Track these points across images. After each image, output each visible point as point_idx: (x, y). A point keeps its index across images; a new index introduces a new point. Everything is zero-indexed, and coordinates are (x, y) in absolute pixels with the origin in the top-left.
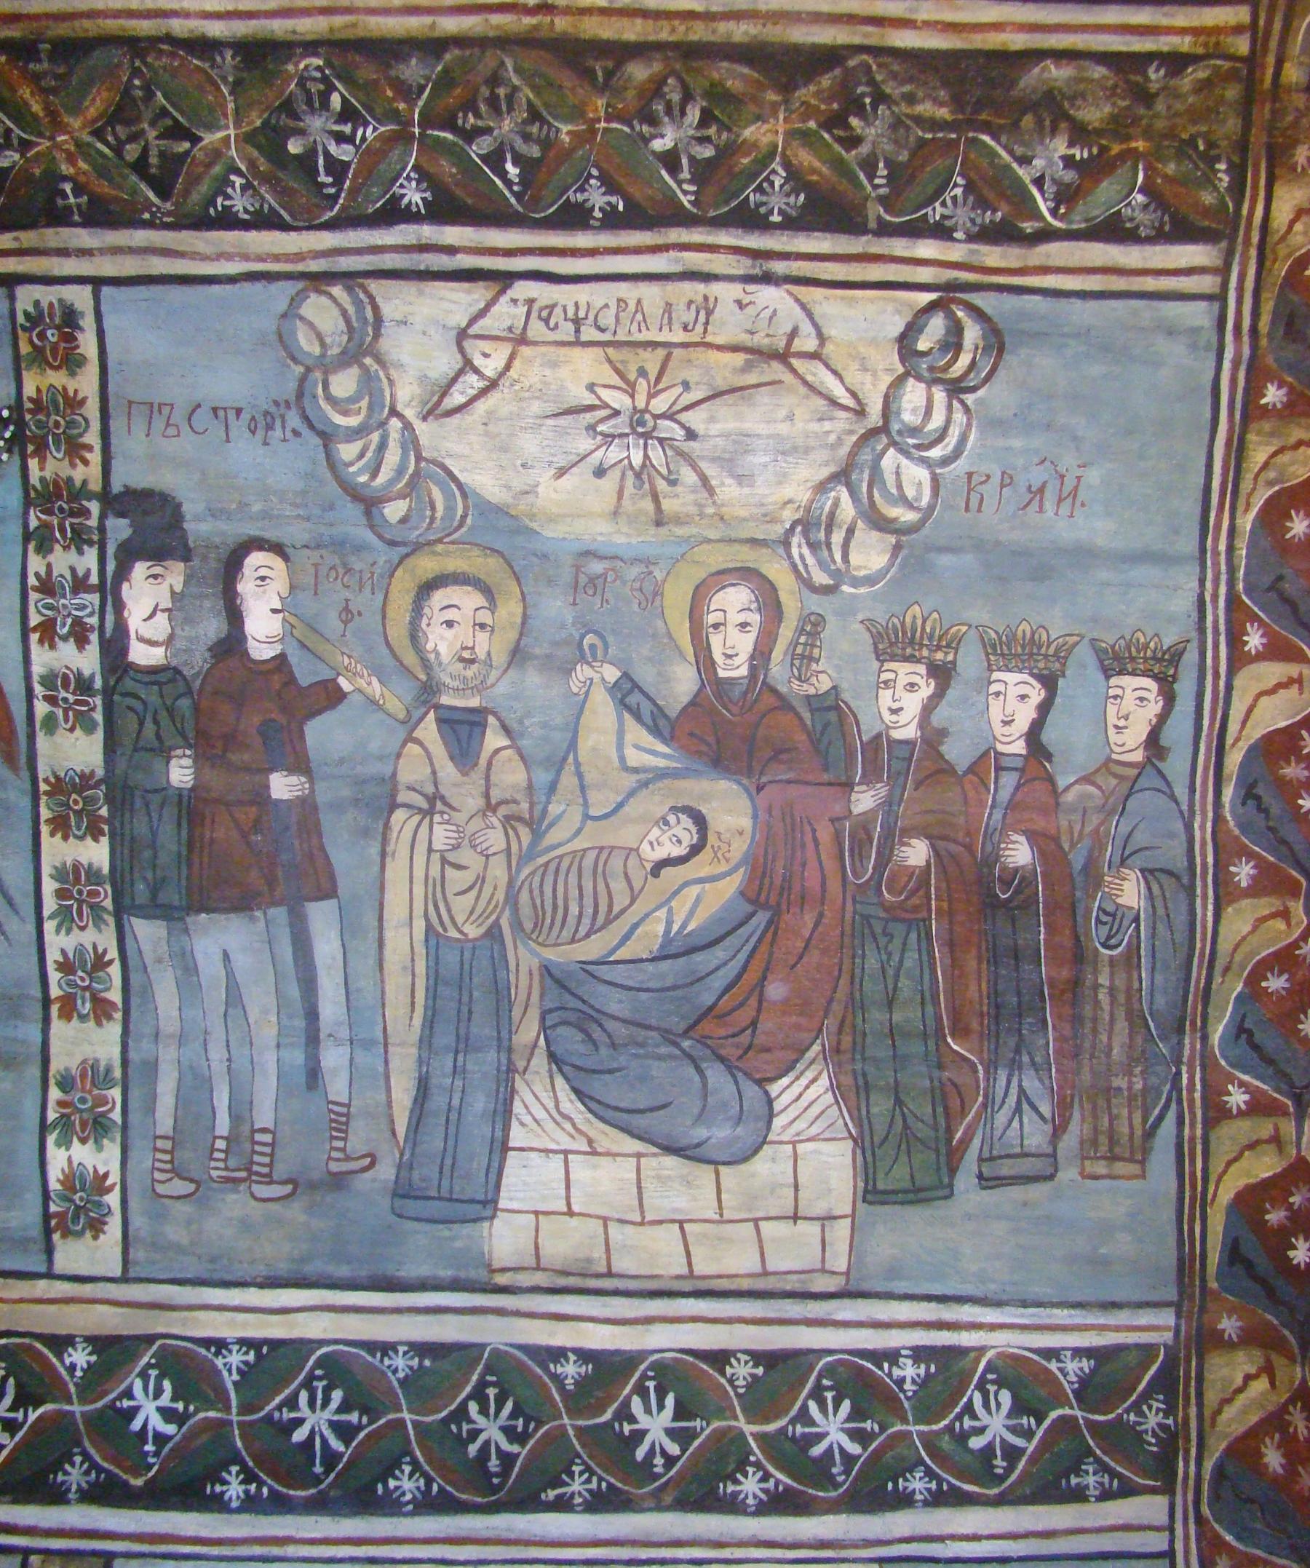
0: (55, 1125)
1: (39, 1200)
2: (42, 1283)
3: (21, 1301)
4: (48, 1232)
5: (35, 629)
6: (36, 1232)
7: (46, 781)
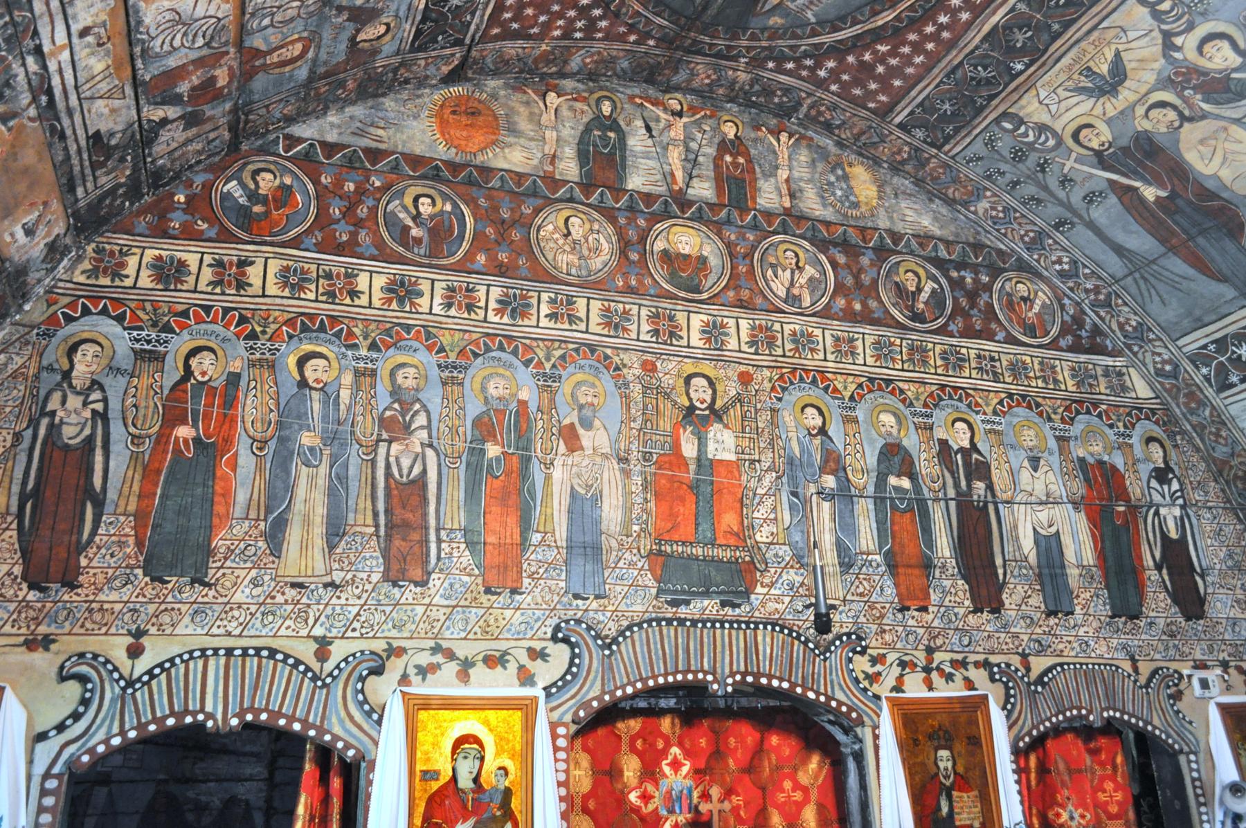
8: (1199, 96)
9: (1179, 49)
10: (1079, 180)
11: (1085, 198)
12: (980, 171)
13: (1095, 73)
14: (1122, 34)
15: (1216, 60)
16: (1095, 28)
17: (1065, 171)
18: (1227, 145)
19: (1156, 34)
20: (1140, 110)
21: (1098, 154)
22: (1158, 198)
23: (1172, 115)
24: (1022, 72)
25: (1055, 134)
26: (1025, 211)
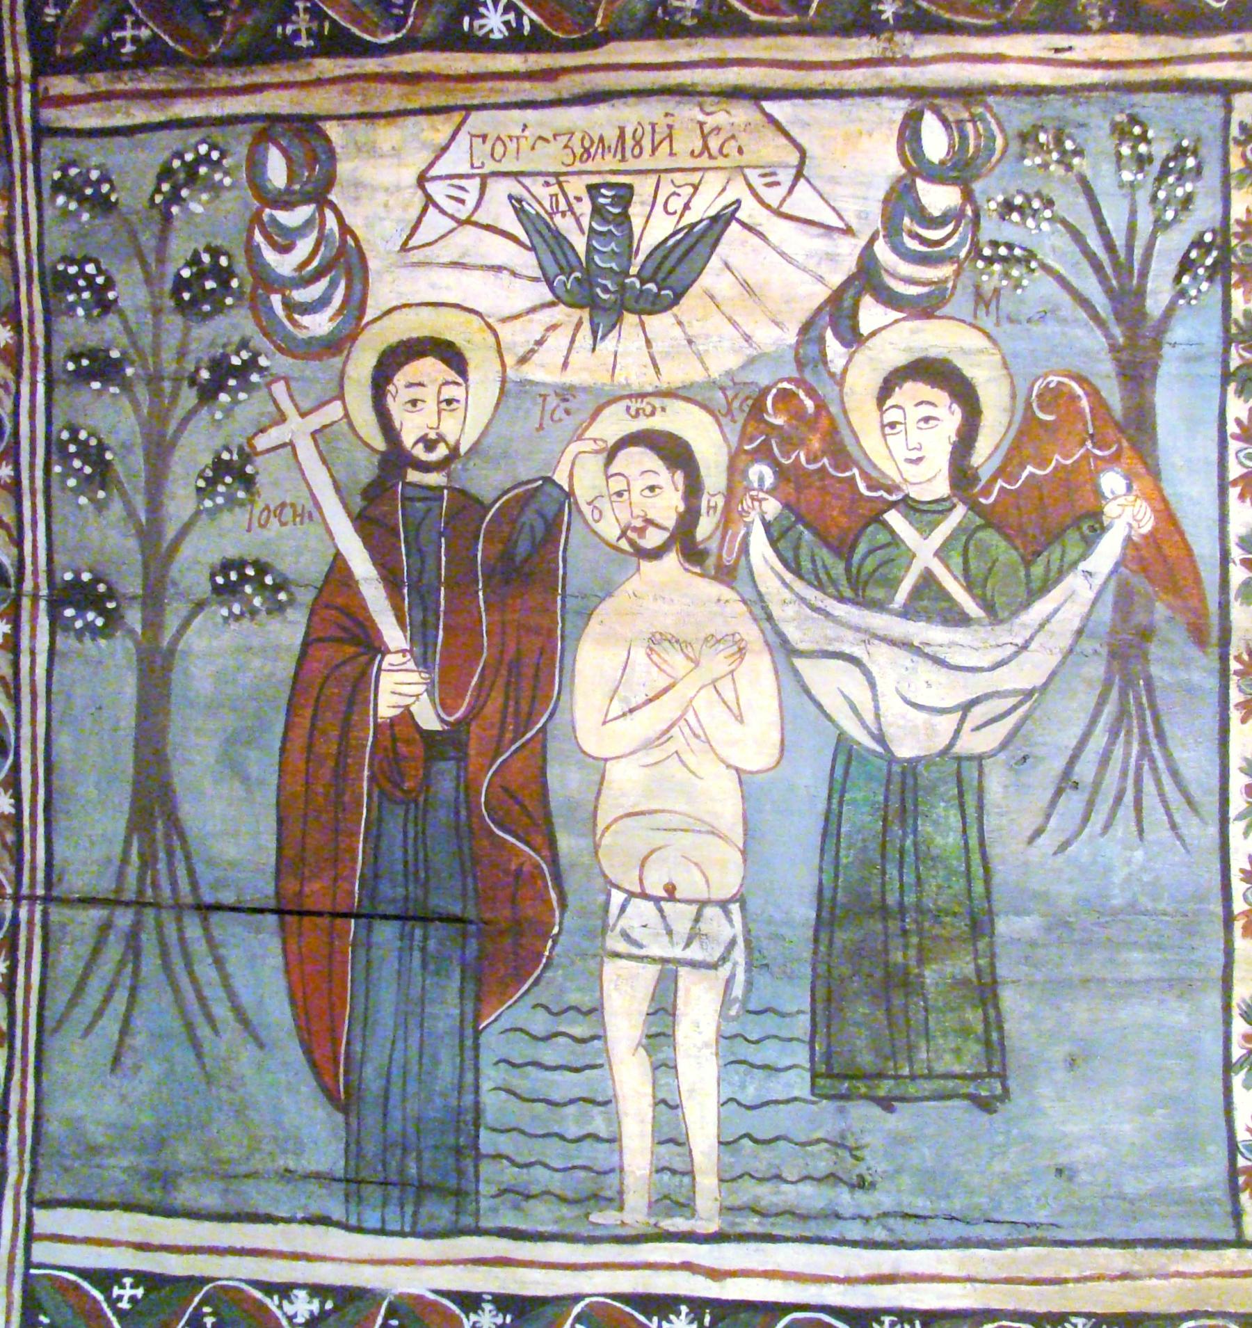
0: (1241, 1063)
1: (1223, 1154)
2: (1231, 1253)
3: (1208, 1274)
4: (1234, 1191)
5: (1235, 483)
6: (1221, 1193)
7: (1238, 659)
8: (772, 507)
9: (853, 338)
10: (268, 494)
11: (226, 567)
12: (58, 243)
13: (624, 220)
14: (786, 177)
15: (896, 441)
16: (757, 95)
17: (262, 442)
18: (705, 703)
19: (848, 252)
20: (614, 424)
21: (395, 459)
22: (407, 716)
23: (668, 505)
24: (485, 45)
25: (355, 306)
26: (33, 477)
